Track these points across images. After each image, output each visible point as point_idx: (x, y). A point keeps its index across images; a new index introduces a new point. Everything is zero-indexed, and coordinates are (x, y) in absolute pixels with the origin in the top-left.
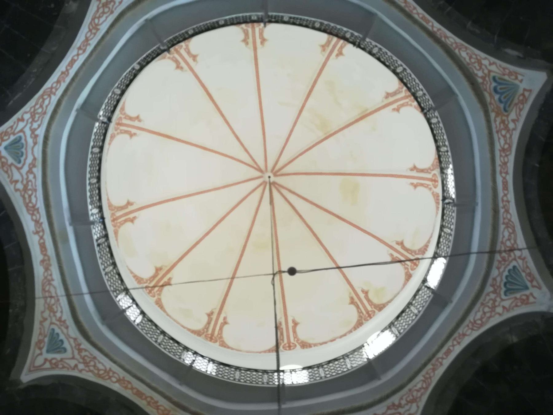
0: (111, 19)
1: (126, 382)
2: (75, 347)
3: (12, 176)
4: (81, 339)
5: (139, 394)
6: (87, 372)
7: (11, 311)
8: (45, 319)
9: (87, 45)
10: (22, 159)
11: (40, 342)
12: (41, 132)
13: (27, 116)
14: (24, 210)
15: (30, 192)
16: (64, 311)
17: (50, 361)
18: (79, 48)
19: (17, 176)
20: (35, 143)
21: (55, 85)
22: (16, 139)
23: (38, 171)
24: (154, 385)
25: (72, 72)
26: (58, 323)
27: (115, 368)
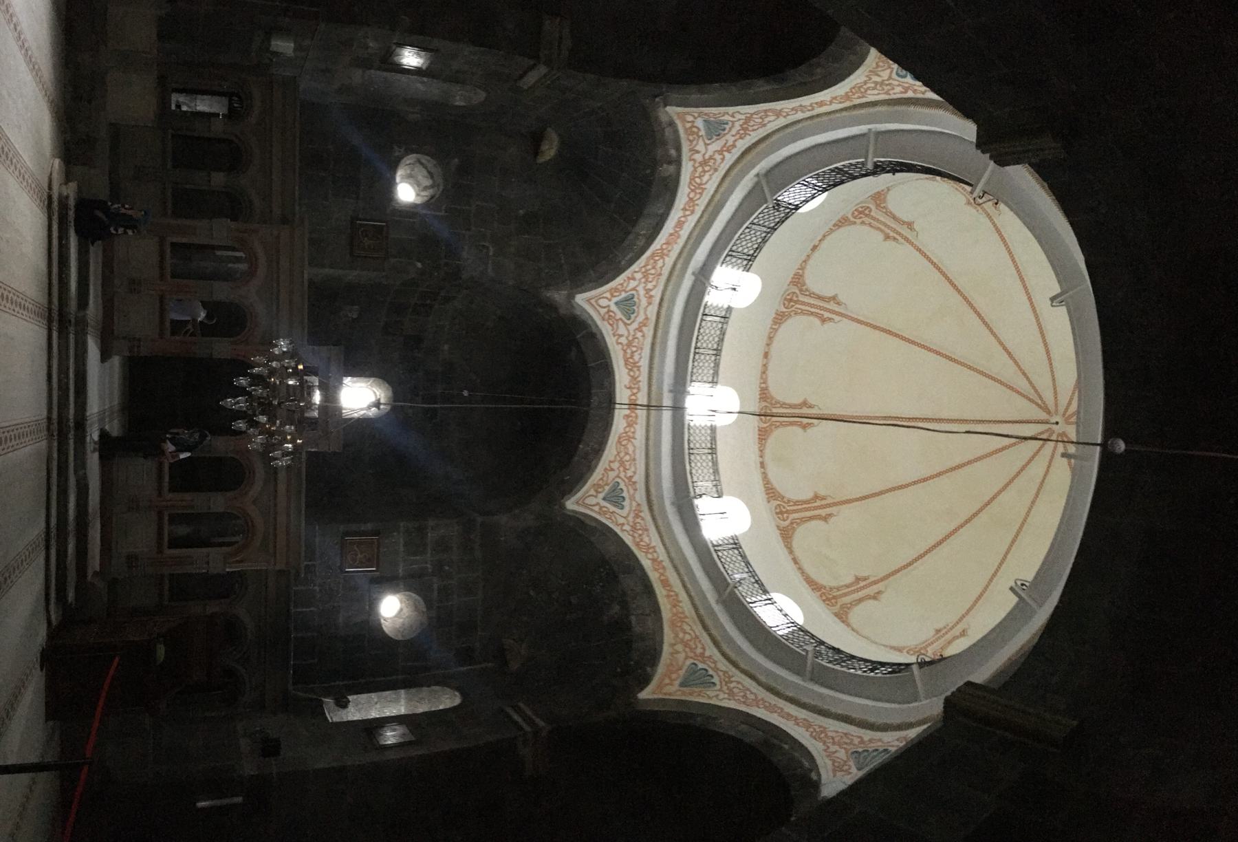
0: (717, 177)
3: (618, 328)
4: (645, 508)
5: (665, 583)
8: (612, 470)
9: (693, 206)
10: (633, 316)
12: (657, 294)
13: (638, 276)
14: (622, 363)
15: (634, 349)
16: (638, 472)
18: (684, 209)
19: (622, 330)
20: (650, 304)
21: (664, 247)
22: (628, 296)
23: (649, 330)
24: (689, 586)
25: (685, 233)
26: (626, 480)
27: (661, 550)
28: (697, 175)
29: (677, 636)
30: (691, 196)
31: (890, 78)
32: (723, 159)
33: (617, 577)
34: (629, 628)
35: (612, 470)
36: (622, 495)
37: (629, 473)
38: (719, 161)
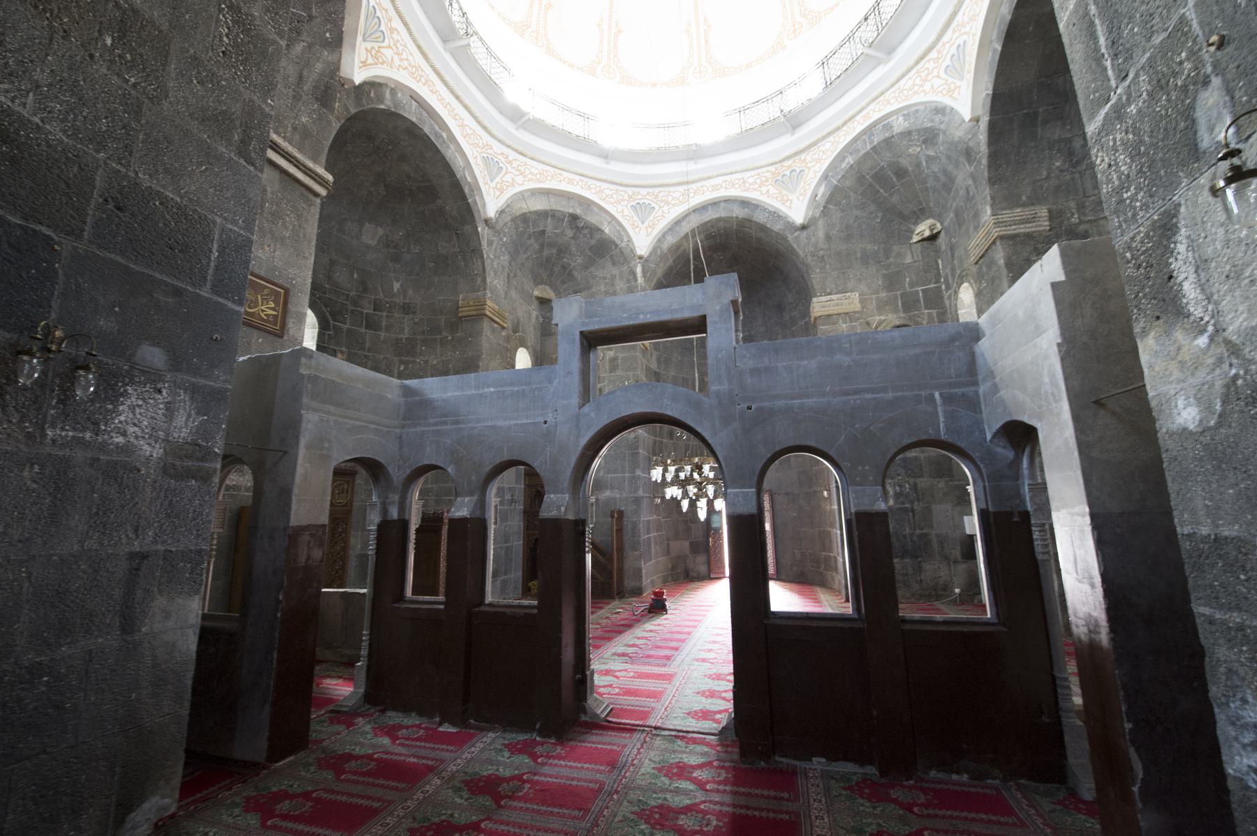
18: (560, 182)
28: (534, 178)
30: (549, 178)
31: (389, 47)
32: (515, 160)
38: (518, 163)
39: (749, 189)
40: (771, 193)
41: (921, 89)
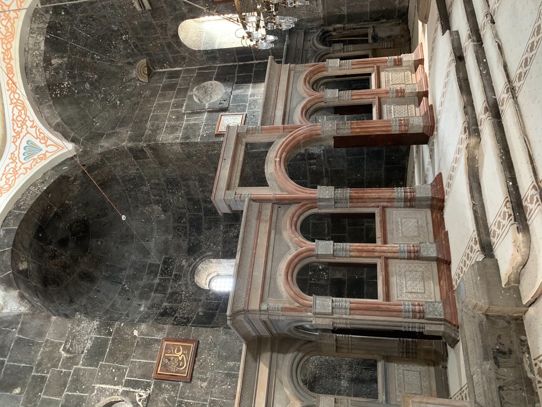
1: (10, 86)
2: (19, 138)
6: (29, 117)
7: (45, 188)
8: (26, 169)
11: (41, 159)
17: (45, 143)
26: (17, 160)
29: (12, 25)
33: (48, 85)
34: (47, 41)
35: (26, 169)
36: (25, 151)
37: (13, 165)
39: (10, 185)
40: (29, 167)
41: (12, 21)
